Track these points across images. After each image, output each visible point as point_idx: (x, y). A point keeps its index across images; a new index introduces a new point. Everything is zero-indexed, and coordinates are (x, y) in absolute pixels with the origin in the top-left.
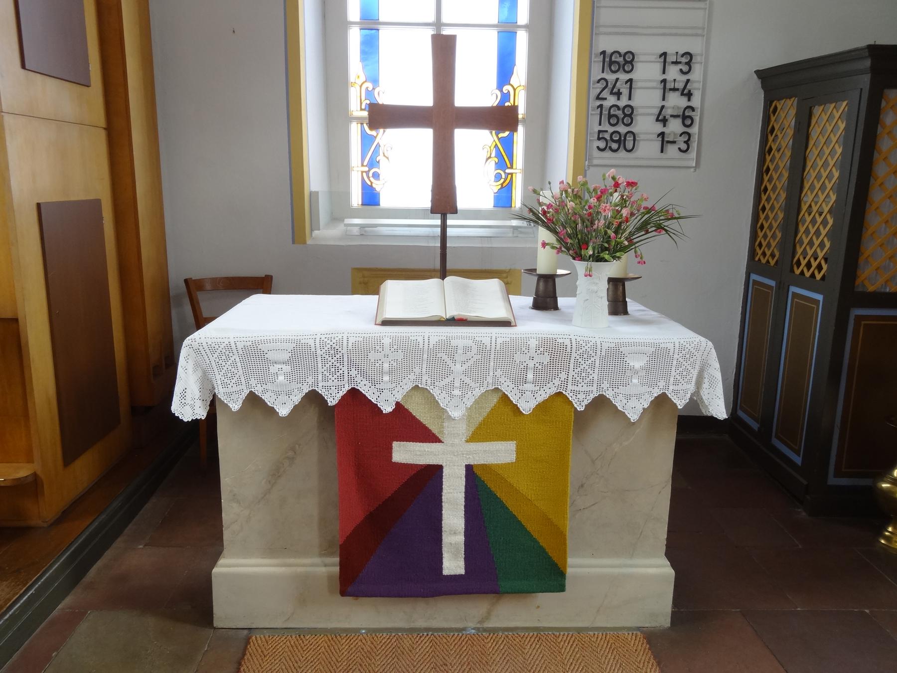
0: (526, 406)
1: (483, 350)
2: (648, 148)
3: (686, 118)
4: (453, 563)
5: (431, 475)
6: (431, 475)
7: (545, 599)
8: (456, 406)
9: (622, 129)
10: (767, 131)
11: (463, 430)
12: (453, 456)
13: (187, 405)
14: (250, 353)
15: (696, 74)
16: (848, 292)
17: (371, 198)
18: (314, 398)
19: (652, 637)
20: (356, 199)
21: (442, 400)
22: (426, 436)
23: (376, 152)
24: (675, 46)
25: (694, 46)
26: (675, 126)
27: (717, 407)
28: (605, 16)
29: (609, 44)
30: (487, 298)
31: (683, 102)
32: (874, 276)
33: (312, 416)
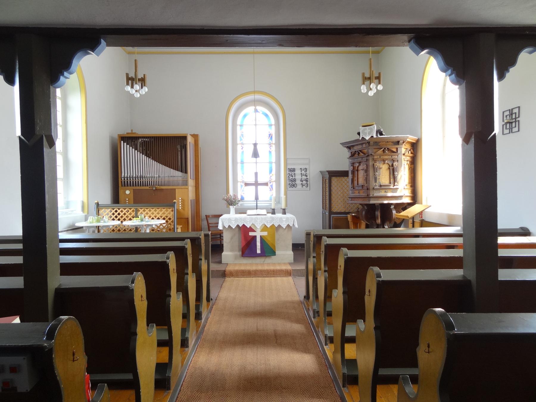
0: (268, 226)
1: (262, 218)
2: (299, 187)
3: (306, 180)
4: (259, 251)
5: (255, 237)
6: (255, 237)
7: (273, 257)
8: (258, 226)
12: (258, 234)
13: (220, 227)
14: (229, 220)
15: (308, 172)
16: (331, 213)
18: (238, 226)
22: (254, 231)
24: (303, 167)
25: (307, 167)
26: (304, 182)
28: (289, 162)
30: (264, 212)
31: (306, 177)
32: (335, 209)
33: (237, 229)
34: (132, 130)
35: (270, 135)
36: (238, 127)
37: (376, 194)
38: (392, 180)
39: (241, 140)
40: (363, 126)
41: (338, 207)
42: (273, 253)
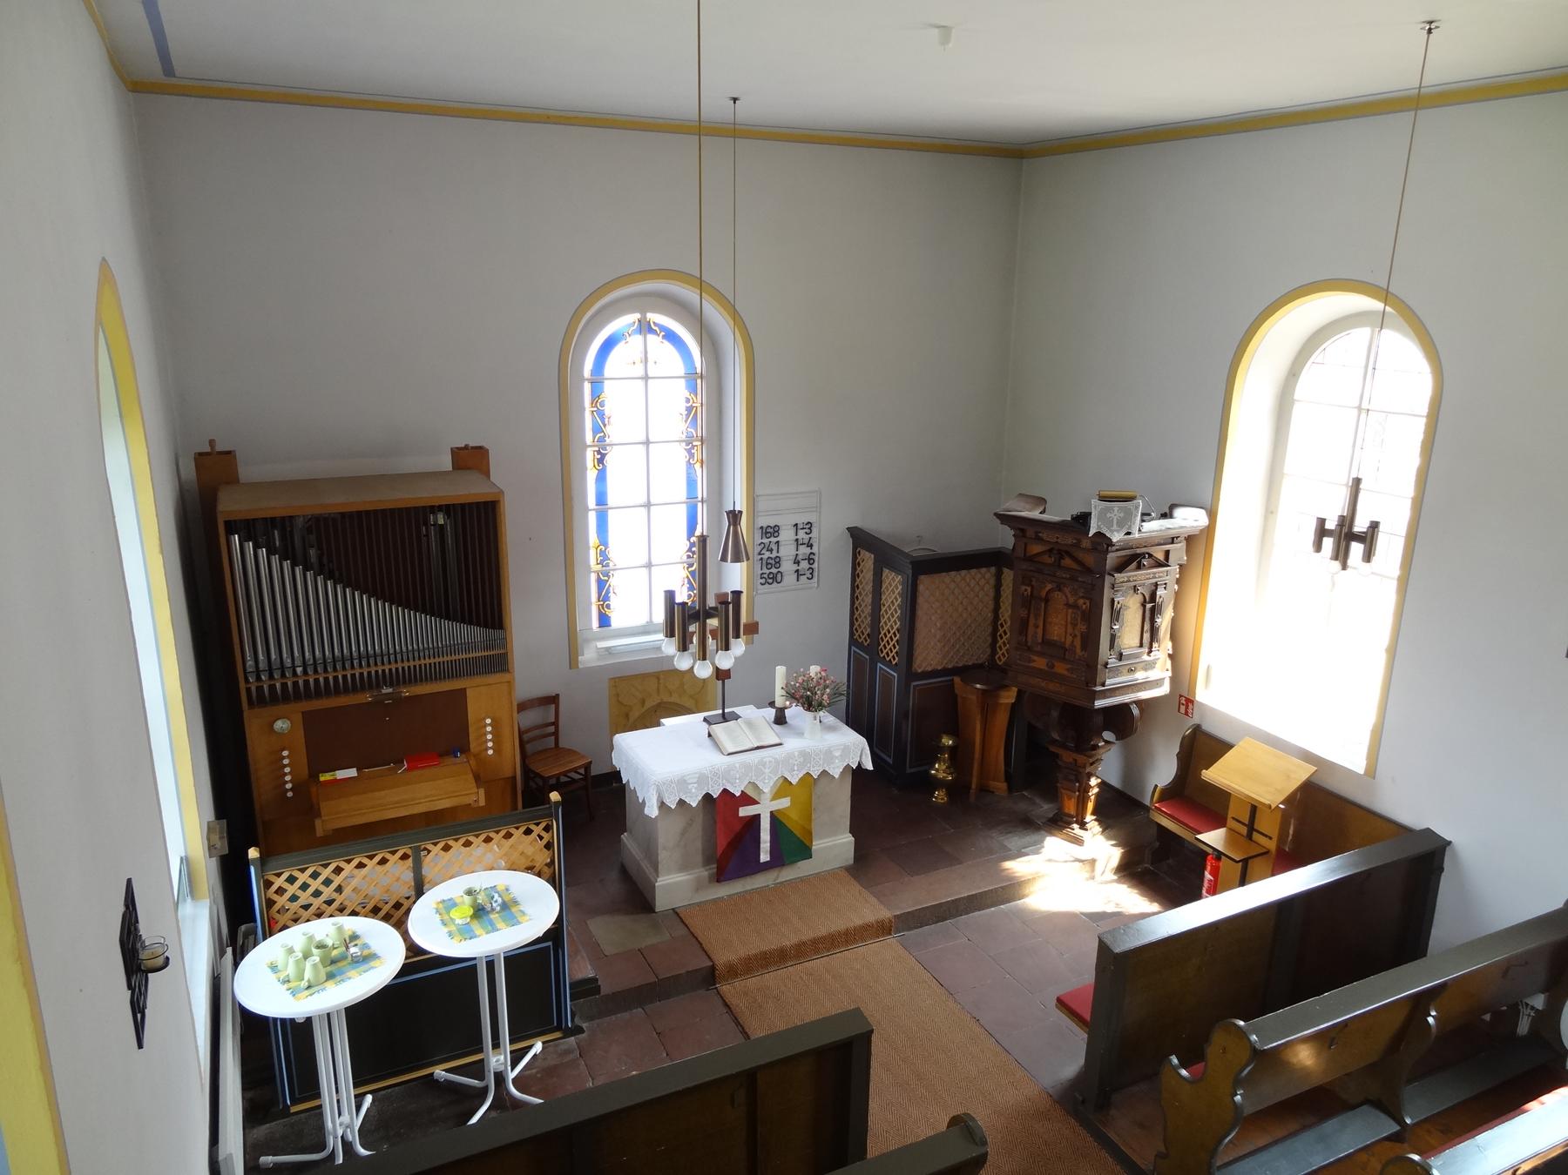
0: (794, 781)
2: (789, 579)
4: (765, 857)
5: (756, 819)
6: (756, 819)
9: (774, 570)
10: (855, 565)
11: (769, 796)
12: (764, 810)
16: (909, 674)
17: (604, 621)
18: (708, 797)
19: (848, 869)
20: (595, 623)
21: (760, 785)
22: (752, 802)
23: (608, 592)
24: (802, 519)
26: (804, 565)
27: (869, 766)
28: (762, 505)
29: (764, 521)
31: (808, 550)
34: (212, 443)
35: (689, 409)
36: (587, 387)
37: (1111, 682)
38: (1147, 636)
39: (597, 430)
40: (1103, 499)
41: (929, 656)
42: (805, 852)
